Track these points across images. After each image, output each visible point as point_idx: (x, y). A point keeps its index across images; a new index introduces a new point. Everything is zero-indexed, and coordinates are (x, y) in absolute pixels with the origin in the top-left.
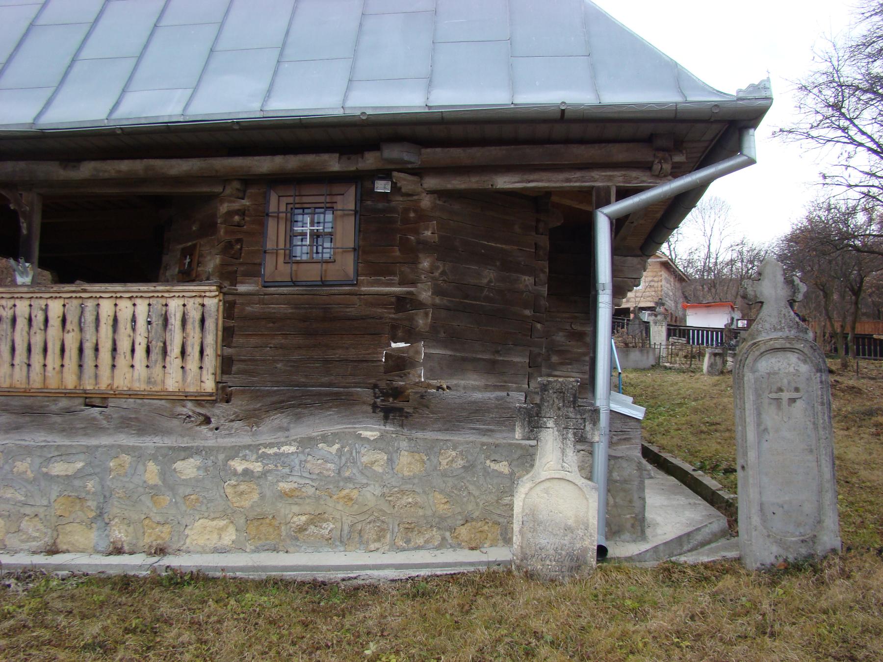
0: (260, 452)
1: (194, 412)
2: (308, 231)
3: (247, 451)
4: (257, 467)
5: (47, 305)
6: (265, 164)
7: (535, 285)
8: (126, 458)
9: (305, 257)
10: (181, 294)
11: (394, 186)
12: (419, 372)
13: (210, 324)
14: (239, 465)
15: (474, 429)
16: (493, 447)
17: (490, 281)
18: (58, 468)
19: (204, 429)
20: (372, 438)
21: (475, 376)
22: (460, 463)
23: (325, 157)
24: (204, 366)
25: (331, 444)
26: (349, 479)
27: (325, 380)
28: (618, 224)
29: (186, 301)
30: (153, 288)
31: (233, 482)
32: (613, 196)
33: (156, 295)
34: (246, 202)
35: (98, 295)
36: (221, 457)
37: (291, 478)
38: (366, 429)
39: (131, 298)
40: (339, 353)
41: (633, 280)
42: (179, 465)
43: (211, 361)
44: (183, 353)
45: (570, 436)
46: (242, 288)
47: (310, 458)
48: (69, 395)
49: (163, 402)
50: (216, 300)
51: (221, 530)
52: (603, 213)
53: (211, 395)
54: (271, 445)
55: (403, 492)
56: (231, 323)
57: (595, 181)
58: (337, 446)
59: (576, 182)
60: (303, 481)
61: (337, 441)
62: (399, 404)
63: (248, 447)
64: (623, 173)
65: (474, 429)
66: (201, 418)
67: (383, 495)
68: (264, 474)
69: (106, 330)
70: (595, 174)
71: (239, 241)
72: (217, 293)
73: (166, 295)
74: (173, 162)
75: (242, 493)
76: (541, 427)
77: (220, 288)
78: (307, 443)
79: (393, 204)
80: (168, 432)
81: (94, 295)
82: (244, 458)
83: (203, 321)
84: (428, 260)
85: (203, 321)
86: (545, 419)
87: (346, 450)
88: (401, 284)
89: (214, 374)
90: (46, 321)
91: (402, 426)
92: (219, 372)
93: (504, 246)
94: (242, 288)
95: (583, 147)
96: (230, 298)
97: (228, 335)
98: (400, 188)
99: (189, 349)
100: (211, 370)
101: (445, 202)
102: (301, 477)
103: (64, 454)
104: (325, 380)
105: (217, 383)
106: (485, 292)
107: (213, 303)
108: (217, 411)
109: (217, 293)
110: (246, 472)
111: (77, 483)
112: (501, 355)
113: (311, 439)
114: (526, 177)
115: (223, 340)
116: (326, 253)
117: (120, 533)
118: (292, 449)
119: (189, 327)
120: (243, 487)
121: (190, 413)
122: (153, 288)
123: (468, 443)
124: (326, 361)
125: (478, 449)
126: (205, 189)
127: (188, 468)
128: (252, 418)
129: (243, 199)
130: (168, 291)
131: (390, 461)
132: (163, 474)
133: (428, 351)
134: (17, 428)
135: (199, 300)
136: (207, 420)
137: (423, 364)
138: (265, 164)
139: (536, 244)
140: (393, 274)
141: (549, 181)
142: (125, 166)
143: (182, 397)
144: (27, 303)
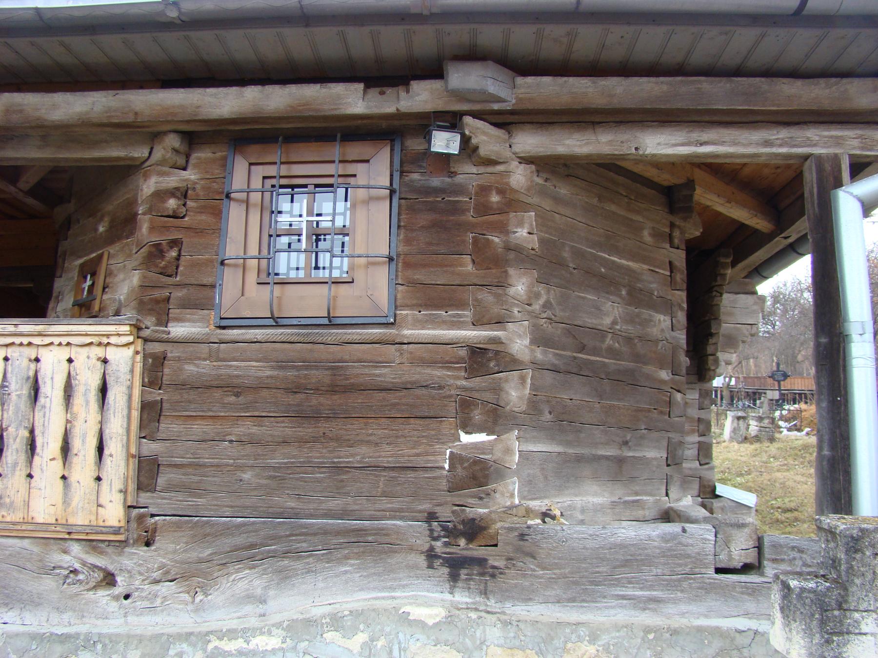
0: (210, 646)
1: (84, 564)
2: (304, 226)
3: (185, 646)
7: (672, 330)
9: (293, 274)
10: (64, 340)
11: (465, 141)
12: (511, 488)
13: (117, 396)
15: (623, 597)
16: (668, 635)
17: (614, 323)
19: (103, 595)
20: (430, 622)
21: (595, 488)
23: (338, 89)
24: (104, 476)
25: (350, 632)
27: (335, 504)
29: (74, 352)
30: (11, 329)
32: (846, 174)
33: (18, 340)
34: (190, 175)
38: (416, 601)
40: (362, 454)
41: (749, 327)
44: (66, 449)
46: (177, 330)
49: (26, 543)
50: (130, 352)
52: (851, 194)
53: (117, 531)
54: (232, 634)
56: (156, 395)
57: (815, 145)
58: (362, 637)
59: (781, 146)
61: (362, 627)
62: (477, 551)
63: (187, 637)
64: (859, 132)
65: (623, 597)
66: (98, 576)
70: (813, 133)
71: (175, 243)
72: (131, 339)
73: (37, 341)
74: (59, 98)
76: (848, 633)
77: (137, 328)
79: (459, 179)
80: (33, 602)
83: (104, 390)
84: (524, 280)
85: (104, 390)
86: (856, 615)
87: (380, 644)
88: (476, 323)
89: (124, 492)
91: (485, 593)
92: (132, 487)
93: (630, 264)
94: (177, 330)
95: (799, 83)
96: (157, 348)
98: (476, 148)
99: (76, 444)
100: (118, 485)
101: (546, 180)
104: (335, 504)
106: (609, 341)
108: (127, 562)
109: (131, 339)
112: (630, 449)
113: (309, 623)
114: (696, 135)
115: (141, 427)
116: (342, 262)
119: (78, 400)
121: (77, 566)
122: (11, 329)
123: (617, 627)
124: (337, 469)
125: (639, 640)
126: (115, 152)
129: (185, 169)
130: (40, 334)
133: (525, 447)
135: (99, 352)
136: (109, 580)
137: (517, 473)
139: (670, 263)
140: (461, 304)
141: (735, 143)
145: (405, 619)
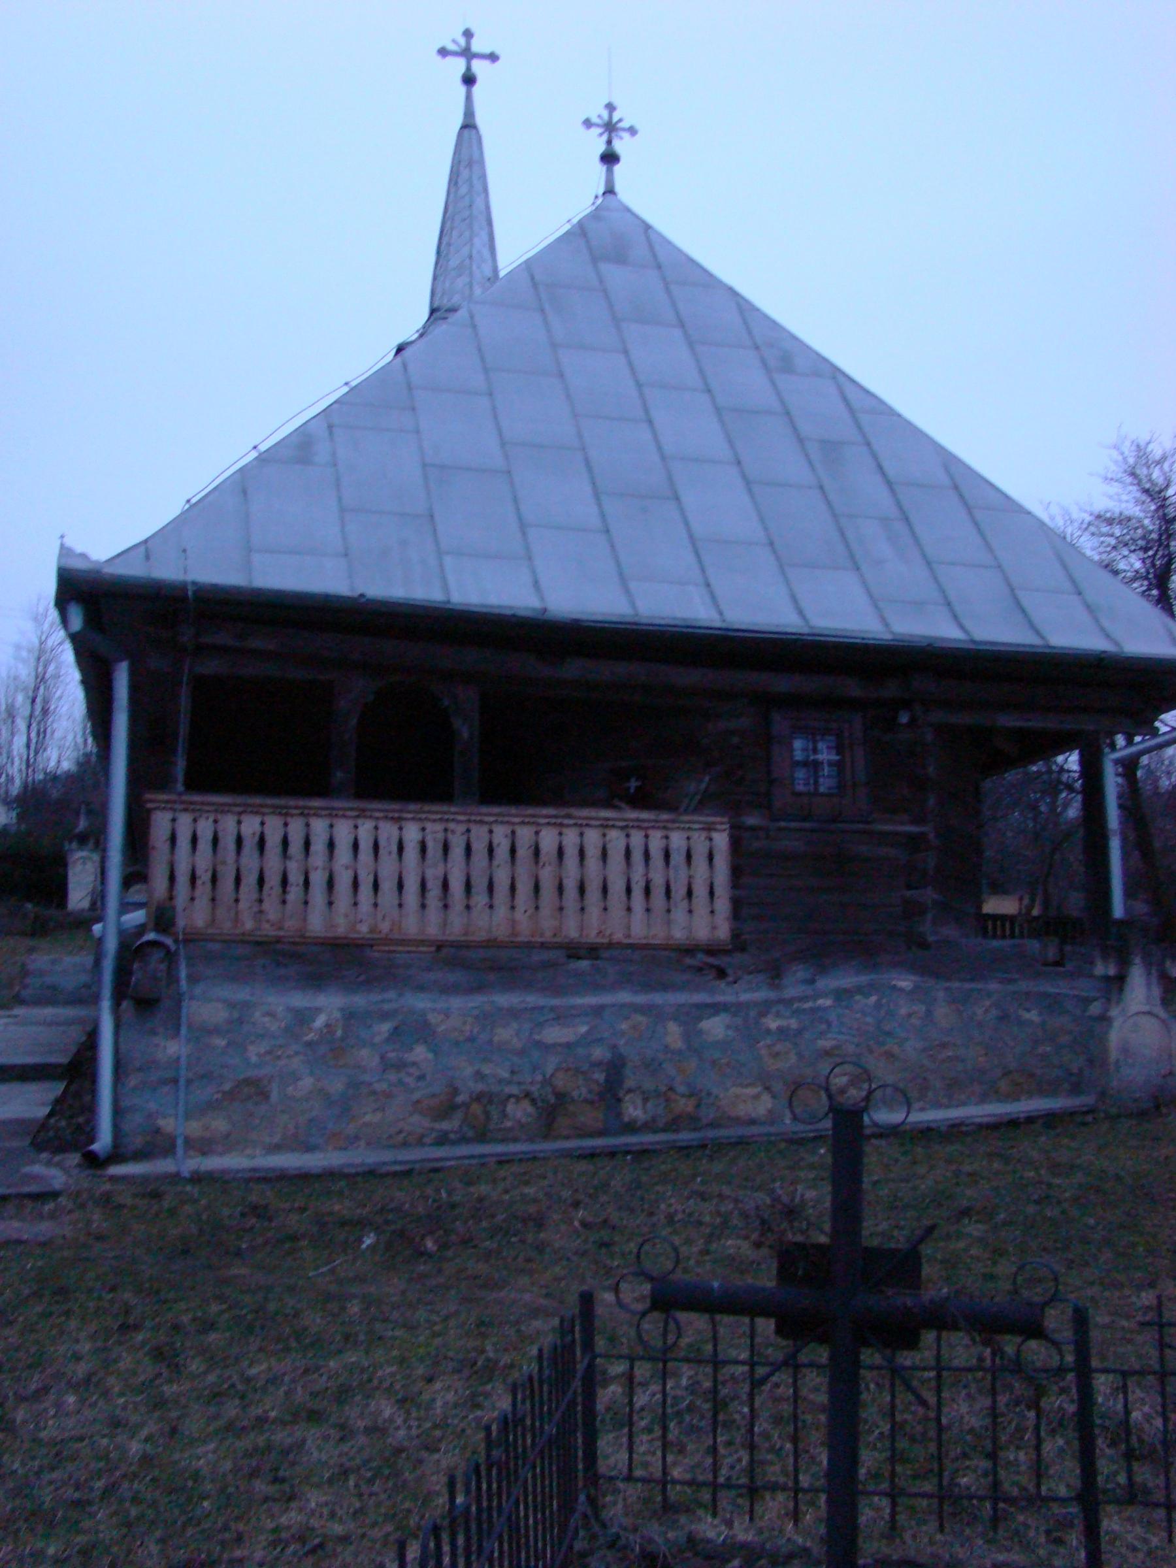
4: (794, 1023)
5: (513, 832)
6: (782, 684)
8: (639, 1018)
10: (687, 826)
14: (773, 1024)
18: (554, 1034)
22: (994, 1012)
26: (889, 1034)
31: (769, 1042)
35: (584, 822)
36: (753, 1014)
37: (829, 1036)
39: (622, 828)
42: (705, 1025)
43: (723, 905)
45: (1153, 971)
47: (847, 1011)
51: (757, 1097)
55: (944, 1046)
58: (873, 999)
60: (841, 1037)
67: (924, 1050)
68: (799, 1032)
69: (593, 863)
73: (669, 825)
75: (777, 1054)
78: (842, 996)
81: (580, 822)
82: (778, 1015)
83: (711, 857)
90: (513, 851)
102: (840, 1033)
103: (561, 1017)
105: (732, 930)
107: (721, 840)
110: (780, 1030)
111: (581, 1051)
113: (846, 991)
117: (635, 1108)
118: (828, 1002)
120: (778, 1047)
127: (715, 1027)
131: (929, 1012)
132: (687, 1036)
134: (480, 988)
136: (721, 973)
138: (782, 684)
142: (621, 670)
143: (689, 950)
144: (485, 828)
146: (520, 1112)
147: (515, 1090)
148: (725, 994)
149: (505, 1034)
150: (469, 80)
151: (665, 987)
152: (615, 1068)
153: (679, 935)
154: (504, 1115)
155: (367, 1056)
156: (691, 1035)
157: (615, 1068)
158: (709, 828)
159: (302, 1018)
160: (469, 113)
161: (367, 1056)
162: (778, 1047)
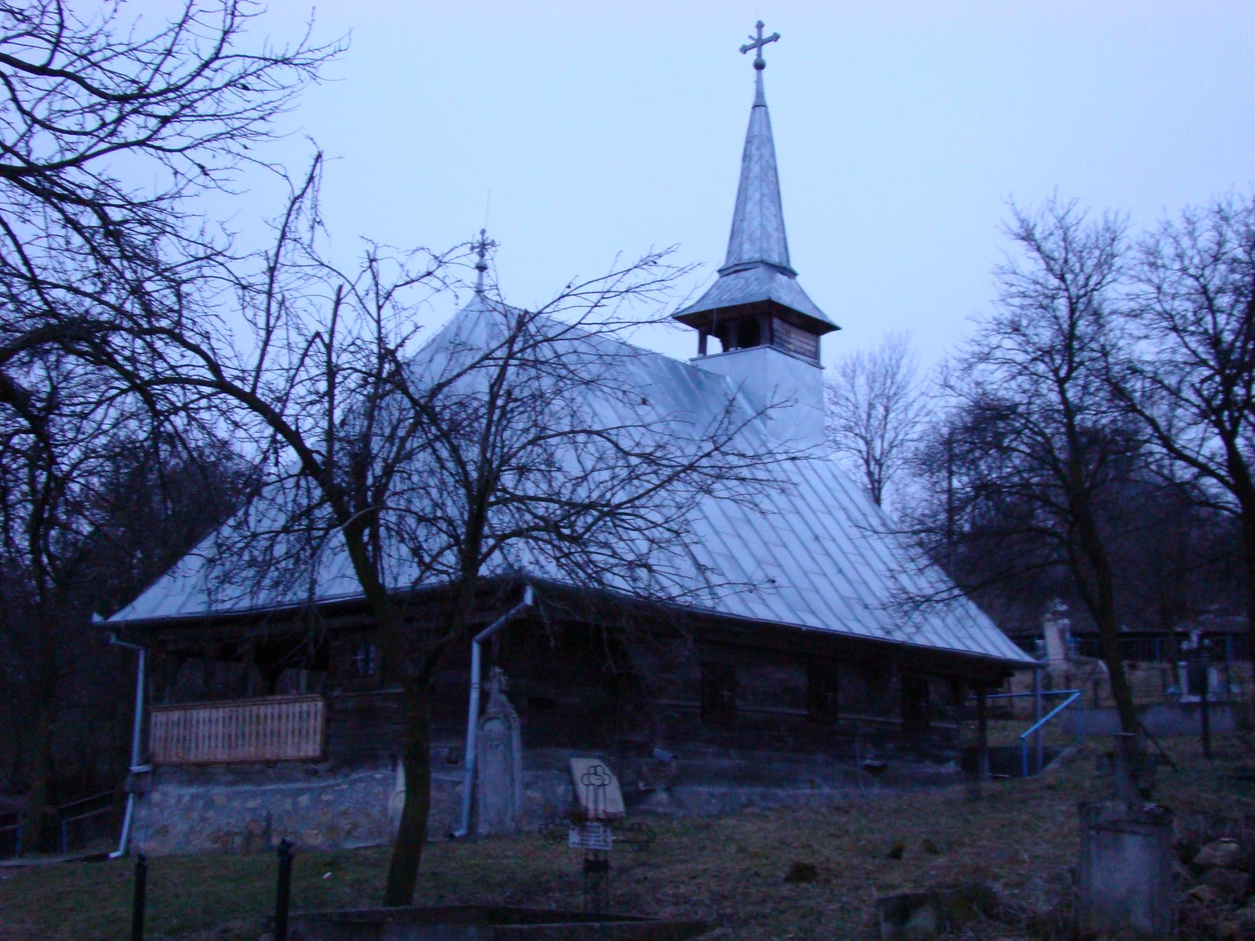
14: (325, 797)
28: (486, 646)
48: (260, 762)
97: (328, 721)
103: (254, 795)
107: (320, 704)
120: (325, 810)
127: (304, 800)
128: (333, 771)
136: (316, 772)
143: (305, 761)
145: (374, 779)
146: (238, 840)
147: (237, 830)
148: (315, 784)
149: (236, 804)
150: (759, 66)
151: (295, 780)
152: (269, 819)
153: (302, 754)
154: (233, 842)
155: (195, 815)
156: (295, 804)
157: (269, 819)
158: (313, 700)
159: (180, 797)
160: (760, 94)
161: (195, 815)
162: (325, 810)
